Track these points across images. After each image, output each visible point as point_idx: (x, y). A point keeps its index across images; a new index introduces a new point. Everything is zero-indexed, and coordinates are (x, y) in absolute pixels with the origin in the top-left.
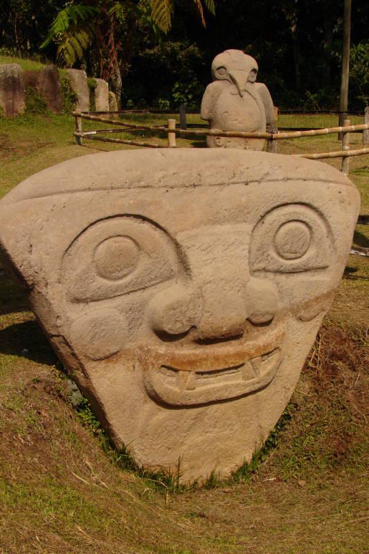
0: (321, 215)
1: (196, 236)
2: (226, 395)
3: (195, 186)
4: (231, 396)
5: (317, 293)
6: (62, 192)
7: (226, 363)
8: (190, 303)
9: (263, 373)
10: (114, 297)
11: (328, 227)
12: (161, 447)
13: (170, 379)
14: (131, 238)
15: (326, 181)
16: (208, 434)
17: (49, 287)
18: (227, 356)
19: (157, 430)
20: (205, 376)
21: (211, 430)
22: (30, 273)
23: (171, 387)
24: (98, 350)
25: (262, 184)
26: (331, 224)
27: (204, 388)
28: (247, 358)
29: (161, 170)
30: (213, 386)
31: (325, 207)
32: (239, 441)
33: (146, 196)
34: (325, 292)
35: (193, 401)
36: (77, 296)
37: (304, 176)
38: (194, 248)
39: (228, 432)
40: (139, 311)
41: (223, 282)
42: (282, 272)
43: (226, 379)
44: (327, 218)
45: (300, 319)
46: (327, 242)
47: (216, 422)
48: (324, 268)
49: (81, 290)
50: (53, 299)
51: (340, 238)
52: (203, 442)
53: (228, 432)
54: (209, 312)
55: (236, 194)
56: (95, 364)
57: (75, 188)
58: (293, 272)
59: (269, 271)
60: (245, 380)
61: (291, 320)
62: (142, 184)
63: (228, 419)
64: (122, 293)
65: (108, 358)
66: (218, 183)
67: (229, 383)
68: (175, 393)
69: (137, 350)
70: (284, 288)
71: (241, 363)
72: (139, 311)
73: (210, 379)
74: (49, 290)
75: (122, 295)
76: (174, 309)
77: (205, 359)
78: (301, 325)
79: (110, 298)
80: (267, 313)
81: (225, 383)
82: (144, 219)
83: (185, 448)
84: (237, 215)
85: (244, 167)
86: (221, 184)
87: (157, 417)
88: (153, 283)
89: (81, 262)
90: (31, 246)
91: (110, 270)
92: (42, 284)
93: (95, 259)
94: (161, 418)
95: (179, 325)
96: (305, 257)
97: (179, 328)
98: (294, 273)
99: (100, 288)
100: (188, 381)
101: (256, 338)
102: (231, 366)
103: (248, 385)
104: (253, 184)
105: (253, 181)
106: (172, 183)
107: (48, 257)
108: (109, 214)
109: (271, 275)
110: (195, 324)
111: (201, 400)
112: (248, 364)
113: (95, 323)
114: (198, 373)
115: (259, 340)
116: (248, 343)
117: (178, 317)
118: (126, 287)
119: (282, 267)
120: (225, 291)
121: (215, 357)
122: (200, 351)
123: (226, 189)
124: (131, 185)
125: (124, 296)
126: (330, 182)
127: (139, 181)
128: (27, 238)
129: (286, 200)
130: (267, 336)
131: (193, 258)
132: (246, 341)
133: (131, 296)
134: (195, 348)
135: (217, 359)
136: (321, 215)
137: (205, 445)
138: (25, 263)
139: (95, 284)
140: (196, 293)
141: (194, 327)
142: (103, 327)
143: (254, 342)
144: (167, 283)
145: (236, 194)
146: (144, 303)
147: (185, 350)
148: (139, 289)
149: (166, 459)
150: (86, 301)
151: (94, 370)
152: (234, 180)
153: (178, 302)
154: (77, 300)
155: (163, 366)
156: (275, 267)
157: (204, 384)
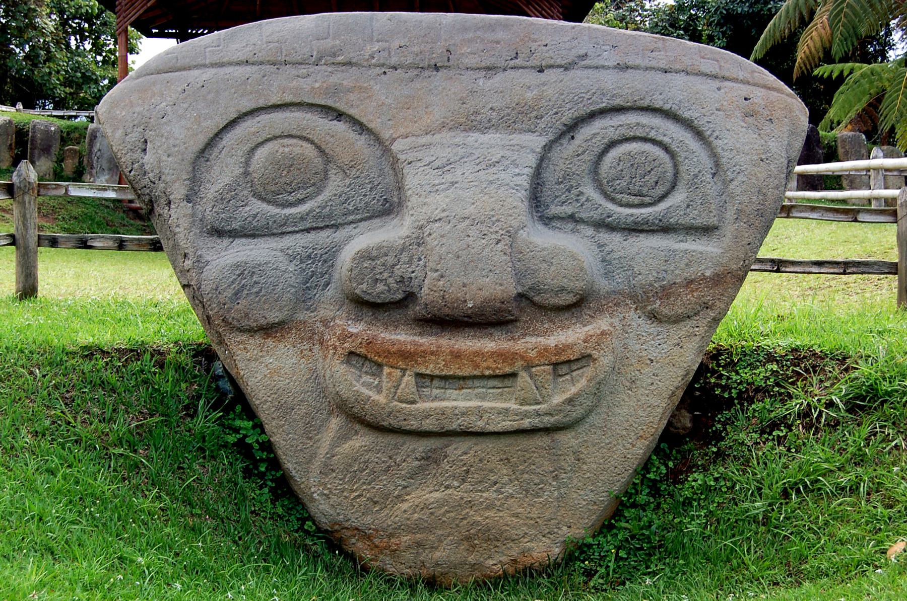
0: (699, 134)
1: (429, 145)
2: (480, 425)
3: (437, 68)
4: (491, 428)
5: (692, 272)
6: (205, 66)
7: (477, 366)
8: (403, 250)
9: (557, 399)
10: (283, 233)
11: (714, 155)
12: (359, 496)
13: (367, 379)
14: (312, 142)
15: (715, 77)
16: (450, 491)
17: (172, 206)
18: (477, 353)
19: (350, 466)
20: (436, 382)
21: (456, 483)
22: (145, 181)
23: (370, 393)
24: (247, 315)
25: (571, 73)
26: (719, 150)
27: (436, 404)
28: (519, 363)
29: (378, 41)
30: (455, 404)
31: (706, 119)
32: (516, 515)
33: (344, 78)
34: (708, 273)
35: (414, 424)
36: (216, 224)
37: (663, 64)
38: (419, 164)
39: (491, 495)
40: (325, 261)
41: (467, 222)
42: (612, 228)
43: (483, 398)
44: (711, 139)
45: (654, 317)
46: (711, 187)
47: (467, 472)
48: (707, 230)
49: (222, 216)
50: (177, 226)
51: (741, 178)
52: (441, 503)
53: (491, 495)
54: (437, 271)
55: (521, 85)
56: (255, 341)
57: (225, 60)
58: (635, 229)
59: (580, 221)
60: (521, 405)
61: (632, 312)
62: (340, 59)
63: (491, 471)
64: (297, 229)
65: (268, 330)
66: (483, 64)
67: (486, 404)
68: (376, 403)
69: (318, 324)
70: (616, 255)
71: (508, 370)
72: (325, 261)
73: (449, 391)
74: (172, 212)
75: (297, 232)
76: (372, 259)
77: (432, 353)
78: (653, 328)
79: (274, 234)
80: (563, 289)
81: (480, 404)
82: (340, 115)
83: (405, 506)
84: (515, 118)
85: (539, 43)
86: (488, 69)
87: (351, 443)
88: (351, 218)
89: (223, 172)
90: (146, 141)
91: (273, 188)
92: (163, 201)
93: (251, 170)
94: (357, 445)
95: (381, 287)
96: (662, 206)
97: (382, 293)
98: (634, 230)
99: (255, 216)
100: (403, 386)
101: (546, 333)
102: (487, 373)
103: (526, 415)
104: (551, 71)
105: (551, 67)
106: (394, 60)
107: (170, 159)
108: (274, 100)
109: (590, 231)
110: (415, 290)
111: (428, 425)
112: (524, 378)
113: (242, 271)
114: (418, 375)
115: (552, 338)
116: (528, 339)
117: (381, 273)
118: (302, 219)
119: (609, 217)
120: (471, 238)
121: (451, 352)
122: (427, 341)
123: (498, 79)
124: (320, 59)
125: (298, 235)
126: (724, 78)
127: (334, 55)
128: (140, 129)
129: (618, 102)
130: (570, 332)
131: (413, 179)
132: (524, 335)
133: (311, 236)
134: (421, 334)
135: (457, 356)
136: (699, 134)
137: (443, 510)
138: (136, 166)
139: (248, 208)
140: (414, 236)
141: (410, 297)
142: (255, 279)
143: (539, 339)
144: (377, 222)
145: (521, 85)
146: (333, 252)
147: (403, 337)
148: (327, 226)
149: (368, 519)
150: (234, 234)
151: (241, 346)
152: (518, 62)
153: (379, 248)
154: (218, 232)
155: (351, 353)
156: (595, 215)
157: (436, 398)
